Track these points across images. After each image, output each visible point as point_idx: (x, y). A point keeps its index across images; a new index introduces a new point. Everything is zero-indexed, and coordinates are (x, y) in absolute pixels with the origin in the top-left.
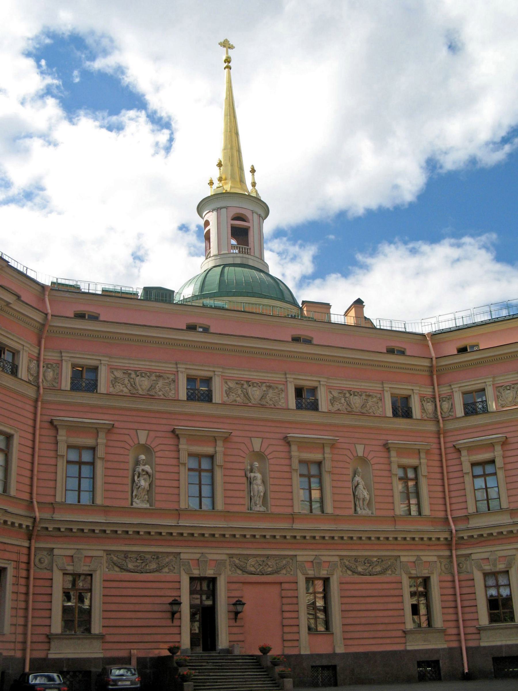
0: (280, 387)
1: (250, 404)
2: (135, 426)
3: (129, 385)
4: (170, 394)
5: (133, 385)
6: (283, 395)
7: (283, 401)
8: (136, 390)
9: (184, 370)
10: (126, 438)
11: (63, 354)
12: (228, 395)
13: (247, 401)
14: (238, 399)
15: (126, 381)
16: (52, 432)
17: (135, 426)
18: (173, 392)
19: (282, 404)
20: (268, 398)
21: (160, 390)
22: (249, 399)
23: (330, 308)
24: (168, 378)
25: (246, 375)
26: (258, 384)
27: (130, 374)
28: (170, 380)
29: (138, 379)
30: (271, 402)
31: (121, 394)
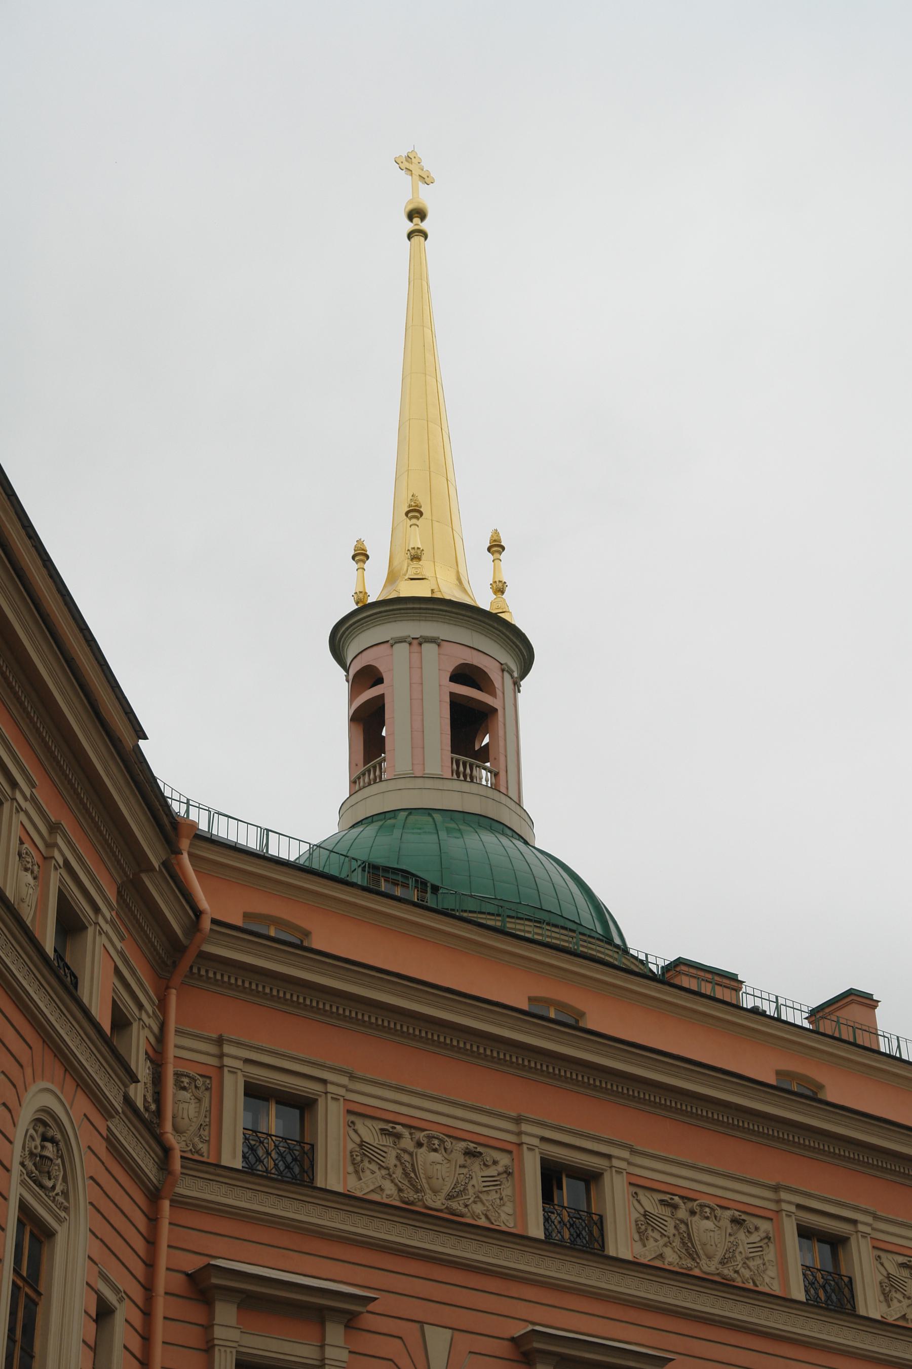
0: (765, 1226)
1: (696, 1272)
2: (416, 1310)
3: (399, 1171)
4: (503, 1217)
5: (410, 1174)
6: (770, 1254)
7: (772, 1272)
8: (417, 1191)
9: (536, 1142)
10: (390, 1348)
11: (227, 1049)
12: (643, 1237)
13: (689, 1263)
14: (668, 1252)
15: (391, 1160)
16: (195, 1313)
17: (416, 1310)
18: (508, 1208)
19: (770, 1283)
20: (739, 1258)
21: (478, 1199)
22: (693, 1255)
23: (876, 1007)
24: (495, 1163)
25: (683, 1179)
26: (712, 1209)
27: (398, 1136)
28: (500, 1168)
29: (425, 1157)
30: (747, 1273)
31: (375, 1197)
